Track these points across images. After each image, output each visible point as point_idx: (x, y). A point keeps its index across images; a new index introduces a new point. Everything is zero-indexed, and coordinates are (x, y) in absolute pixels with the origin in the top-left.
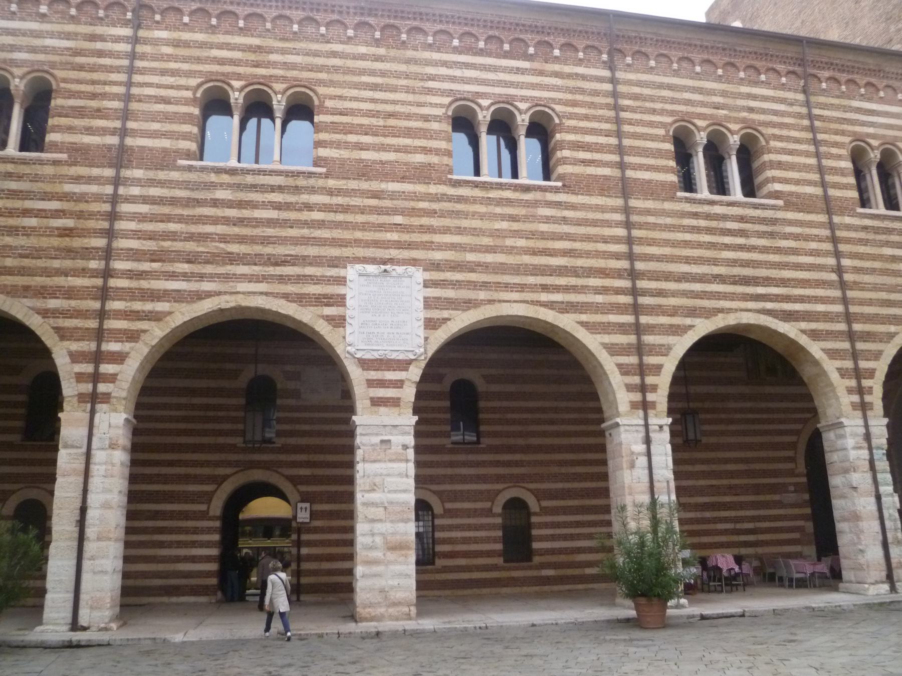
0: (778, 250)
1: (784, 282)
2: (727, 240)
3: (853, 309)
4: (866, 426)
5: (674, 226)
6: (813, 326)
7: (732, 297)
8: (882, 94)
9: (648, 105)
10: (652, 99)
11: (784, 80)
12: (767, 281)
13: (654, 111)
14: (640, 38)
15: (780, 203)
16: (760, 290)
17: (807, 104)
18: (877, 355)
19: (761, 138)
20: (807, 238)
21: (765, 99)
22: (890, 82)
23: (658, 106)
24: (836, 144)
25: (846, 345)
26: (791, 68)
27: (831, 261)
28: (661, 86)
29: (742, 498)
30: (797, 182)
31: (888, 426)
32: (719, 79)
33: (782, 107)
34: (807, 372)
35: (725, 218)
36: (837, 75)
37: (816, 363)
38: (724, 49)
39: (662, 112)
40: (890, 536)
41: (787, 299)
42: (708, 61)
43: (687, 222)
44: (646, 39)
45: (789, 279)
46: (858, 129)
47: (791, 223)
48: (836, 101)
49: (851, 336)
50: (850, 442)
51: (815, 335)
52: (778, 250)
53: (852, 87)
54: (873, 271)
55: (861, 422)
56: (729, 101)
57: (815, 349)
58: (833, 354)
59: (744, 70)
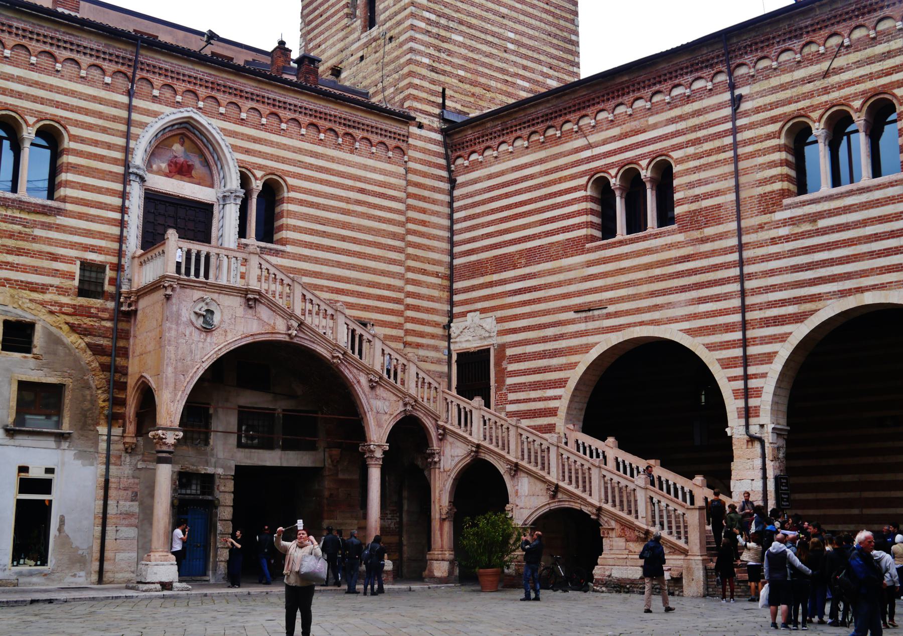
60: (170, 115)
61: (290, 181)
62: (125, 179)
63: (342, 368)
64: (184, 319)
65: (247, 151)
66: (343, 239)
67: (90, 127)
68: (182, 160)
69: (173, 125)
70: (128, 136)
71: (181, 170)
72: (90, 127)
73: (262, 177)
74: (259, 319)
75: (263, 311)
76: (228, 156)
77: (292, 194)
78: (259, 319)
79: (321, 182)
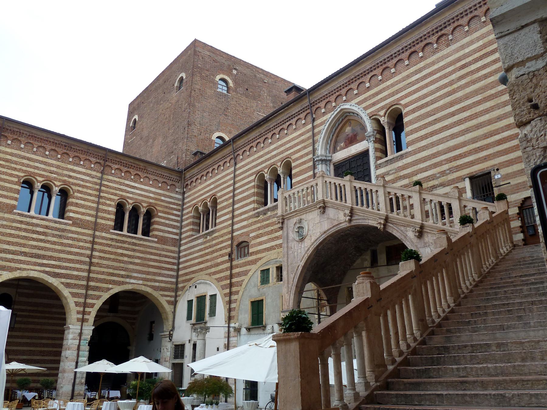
0: (62, 244)
1: (59, 259)
2: (35, 236)
3: (92, 275)
4: (81, 329)
5: (7, 226)
6: (68, 281)
7: (28, 263)
8: (142, 180)
9: (13, 165)
10: (16, 163)
11: (93, 166)
12: (51, 258)
13: (15, 169)
14: (20, 133)
15: (71, 222)
16: (45, 262)
17: (101, 179)
18: (98, 298)
19: (71, 191)
20: (79, 240)
21: (79, 173)
22: (148, 175)
23: (18, 167)
24: (110, 199)
25: (84, 292)
26: (98, 161)
27: (89, 252)
28: (24, 158)
29: (46, 358)
30: (83, 214)
31: (94, 330)
32: (58, 160)
33: (88, 178)
34: (64, 302)
35: (37, 225)
36: (122, 168)
37: (66, 298)
38: (65, 146)
39: (20, 170)
40: (77, 381)
41: (59, 267)
42: (54, 150)
43: (14, 225)
44: (23, 133)
45: (62, 258)
46: (124, 194)
47: (72, 232)
48: (117, 180)
49: (87, 288)
50: (71, 336)
51: (67, 285)
52: (62, 244)
53: (128, 174)
54: (109, 259)
55: (79, 327)
56: (60, 171)
57: (66, 292)
58: (74, 295)
59: (73, 158)
60: (330, 117)
61: (403, 102)
62: (314, 167)
63: (390, 230)
64: (290, 238)
65: (374, 104)
66: (453, 114)
67: (299, 151)
68: (351, 134)
69: (338, 120)
70: (314, 143)
71: (352, 140)
72: (299, 151)
73: (385, 114)
74: (328, 218)
75: (331, 212)
76: (363, 115)
77: (407, 109)
78: (328, 218)
79: (427, 86)
